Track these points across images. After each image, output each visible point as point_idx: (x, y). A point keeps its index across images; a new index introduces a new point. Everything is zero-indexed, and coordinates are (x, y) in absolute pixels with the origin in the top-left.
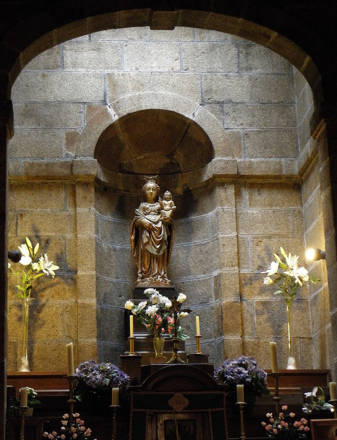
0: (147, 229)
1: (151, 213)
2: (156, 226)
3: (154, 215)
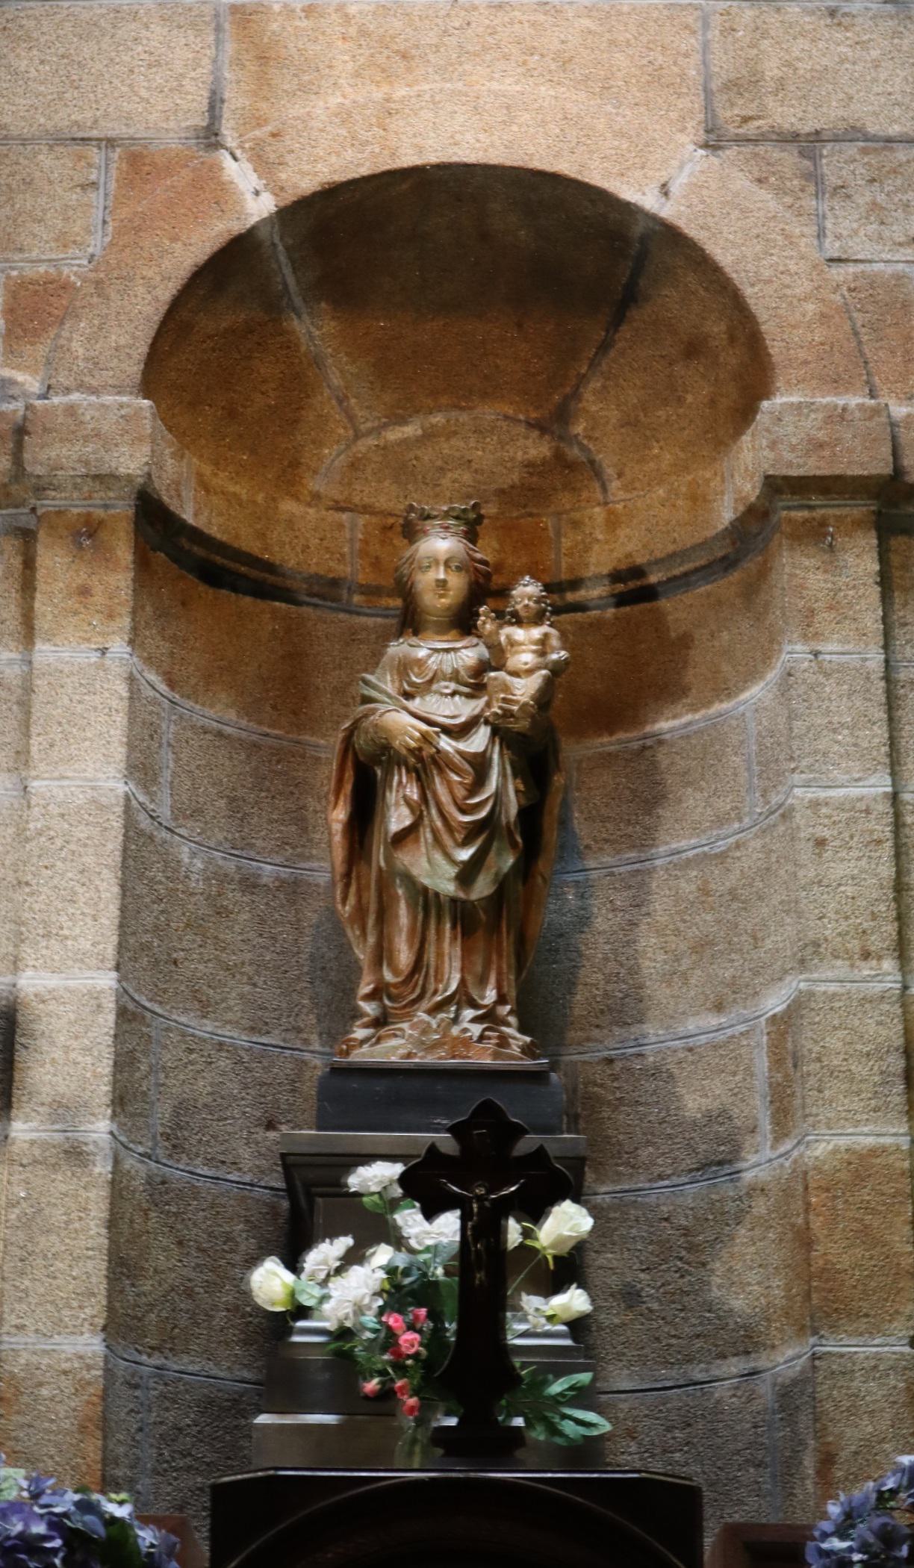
1: (435, 687)
2: (462, 746)
3: (453, 694)
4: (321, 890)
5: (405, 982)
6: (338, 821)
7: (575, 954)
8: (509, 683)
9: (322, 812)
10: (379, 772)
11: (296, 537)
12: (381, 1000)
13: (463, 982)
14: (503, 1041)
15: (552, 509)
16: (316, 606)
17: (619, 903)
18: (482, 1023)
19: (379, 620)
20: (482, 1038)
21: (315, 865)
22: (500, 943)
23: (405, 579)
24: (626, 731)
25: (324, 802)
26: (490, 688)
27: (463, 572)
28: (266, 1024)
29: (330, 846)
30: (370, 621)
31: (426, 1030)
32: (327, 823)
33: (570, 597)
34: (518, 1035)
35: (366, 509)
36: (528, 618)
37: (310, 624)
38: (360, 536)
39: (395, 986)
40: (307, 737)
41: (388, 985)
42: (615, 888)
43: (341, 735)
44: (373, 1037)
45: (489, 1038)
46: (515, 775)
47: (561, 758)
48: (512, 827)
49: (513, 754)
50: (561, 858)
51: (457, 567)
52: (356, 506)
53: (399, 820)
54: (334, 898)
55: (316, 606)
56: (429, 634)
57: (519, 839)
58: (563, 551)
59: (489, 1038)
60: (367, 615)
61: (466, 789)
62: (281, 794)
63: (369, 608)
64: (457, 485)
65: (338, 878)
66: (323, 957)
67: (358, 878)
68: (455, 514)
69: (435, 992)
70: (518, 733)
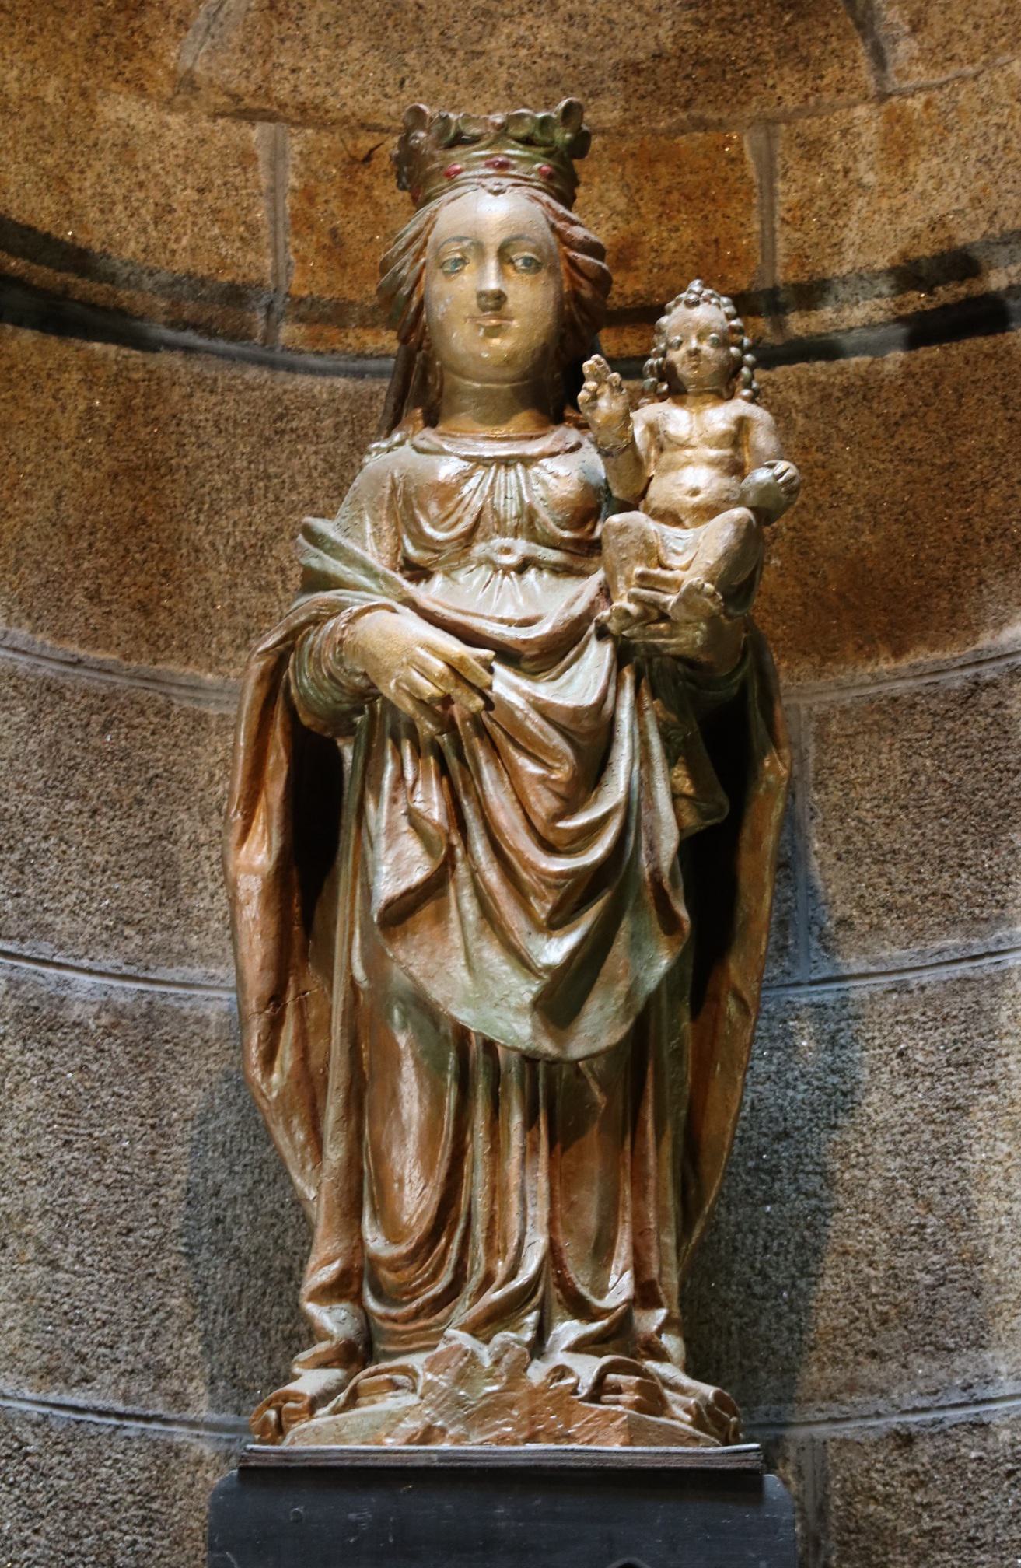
0: (427, 727)
1: (478, 549)
2: (544, 691)
3: (522, 568)
4: (211, 1033)
5: (413, 1256)
6: (251, 870)
7: (817, 1179)
8: (652, 539)
9: (211, 845)
10: (348, 754)
11: (141, 185)
12: (358, 1299)
13: (553, 1254)
14: (652, 1399)
15: (753, 109)
16: (189, 350)
17: (920, 1057)
18: (600, 1355)
19: (341, 382)
20: (600, 1389)
21: (196, 973)
22: (639, 1158)
23: (405, 291)
24: (933, 647)
25: (216, 823)
26: (608, 551)
27: (543, 274)
28: (83, 1358)
29: (232, 926)
30: (320, 387)
31: (467, 1371)
32: (224, 871)
33: (798, 324)
34: (686, 1381)
35: (307, 114)
36: (698, 382)
37: (176, 394)
38: (293, 181)
39: (393, 1265)
40: (173, 667)
41: (374, 1261)
42: (911, 1022)
43: (257, 667)
44: (341, 1388)
45: (618, 1390)
46: (671, 760)
47: (779, 712)
48: (666, 883)
49: (668, 706)
50: (782, 949)
51: (528, 261)
52: (283, 106)
53: (399, 874)
54: (242, 1049)
55: (189, 350)
56: (464, 420)
57: (682, 911)
58: (780, 211)
59: (618, 1390)
60: (312, 371)
61: (556, 794)
62: (112, 804)
63: (318, 353)
64: (523, 52)
65: (253, 1005)
66: (216, 1194)
67: (301, 1007)
68: (522, 132)
69: (488, 1281)
70: (678, 658)
